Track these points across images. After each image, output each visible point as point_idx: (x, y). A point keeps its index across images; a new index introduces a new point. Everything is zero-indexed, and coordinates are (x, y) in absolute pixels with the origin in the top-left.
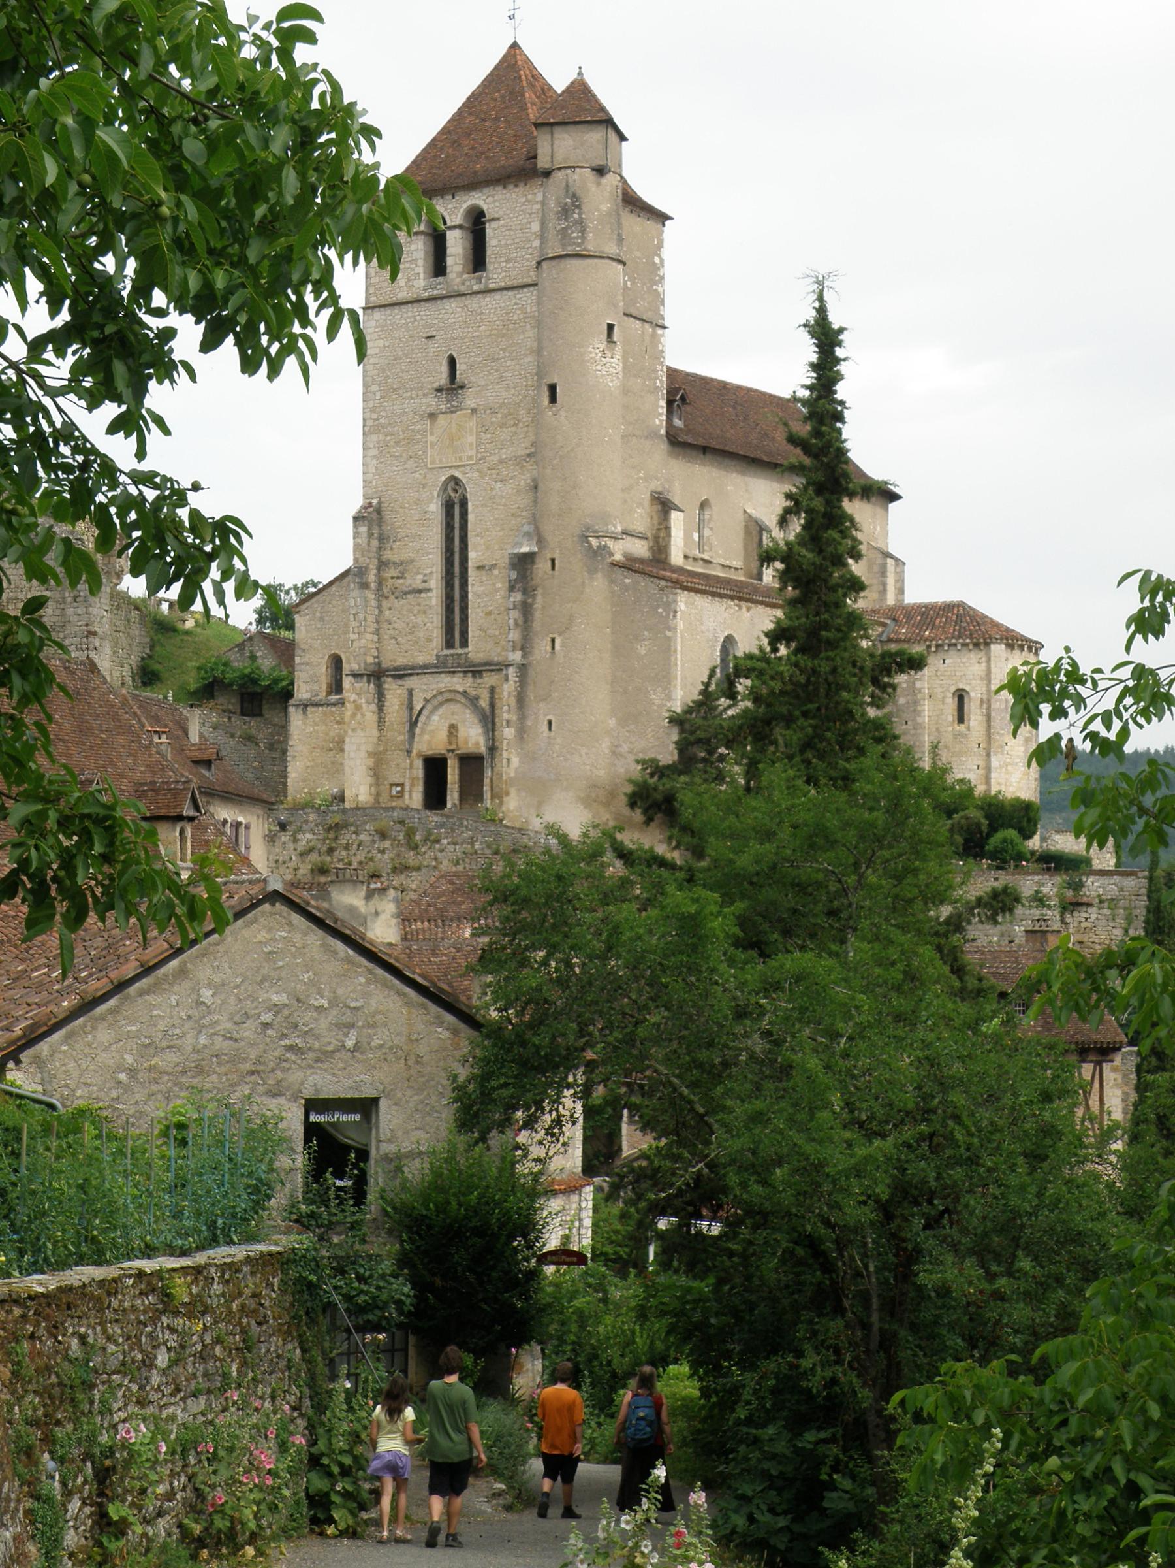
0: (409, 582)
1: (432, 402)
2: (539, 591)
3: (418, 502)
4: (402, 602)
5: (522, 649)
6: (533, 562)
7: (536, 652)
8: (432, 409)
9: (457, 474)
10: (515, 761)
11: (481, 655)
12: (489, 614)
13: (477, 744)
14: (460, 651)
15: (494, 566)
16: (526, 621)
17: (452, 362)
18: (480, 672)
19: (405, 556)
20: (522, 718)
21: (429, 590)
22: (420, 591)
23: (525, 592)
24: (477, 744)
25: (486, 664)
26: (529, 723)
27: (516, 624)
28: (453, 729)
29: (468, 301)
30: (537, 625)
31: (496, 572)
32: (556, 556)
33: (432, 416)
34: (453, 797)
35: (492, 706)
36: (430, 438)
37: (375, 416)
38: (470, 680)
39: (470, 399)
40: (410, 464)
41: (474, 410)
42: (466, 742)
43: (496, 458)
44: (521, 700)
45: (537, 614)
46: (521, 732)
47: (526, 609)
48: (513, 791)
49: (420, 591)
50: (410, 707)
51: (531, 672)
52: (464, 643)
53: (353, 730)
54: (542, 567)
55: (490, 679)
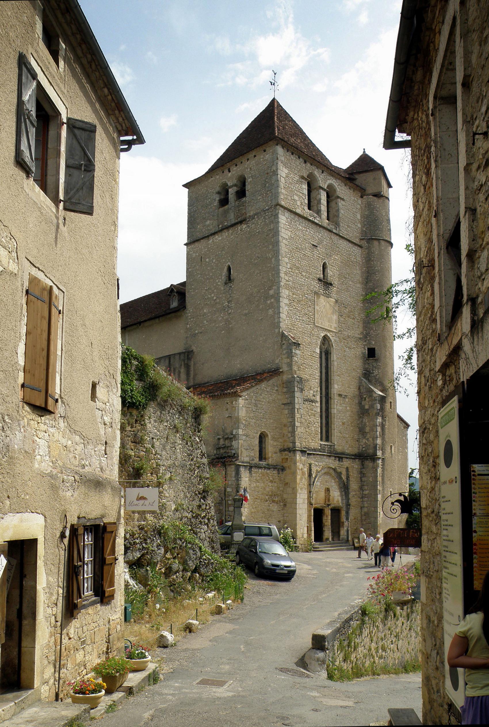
1: (316, 286)
2: (387, 419)
3: (310, 344)
5: (382, 450)
11: (340, 448)
12: (343, 424)
13: (338, 501)
16: (383, 435)
18: (342, 458)
23: (383, 417)
24: (338, 501)
28: (328, 490)
31: (347, 400)
34: (327, 533)
35: (348, 477)
38: (337, 462)
42: (333, 501)
45: (387, 430)
49: (312, 401)
50: (310, 475)
53: (301, 489)
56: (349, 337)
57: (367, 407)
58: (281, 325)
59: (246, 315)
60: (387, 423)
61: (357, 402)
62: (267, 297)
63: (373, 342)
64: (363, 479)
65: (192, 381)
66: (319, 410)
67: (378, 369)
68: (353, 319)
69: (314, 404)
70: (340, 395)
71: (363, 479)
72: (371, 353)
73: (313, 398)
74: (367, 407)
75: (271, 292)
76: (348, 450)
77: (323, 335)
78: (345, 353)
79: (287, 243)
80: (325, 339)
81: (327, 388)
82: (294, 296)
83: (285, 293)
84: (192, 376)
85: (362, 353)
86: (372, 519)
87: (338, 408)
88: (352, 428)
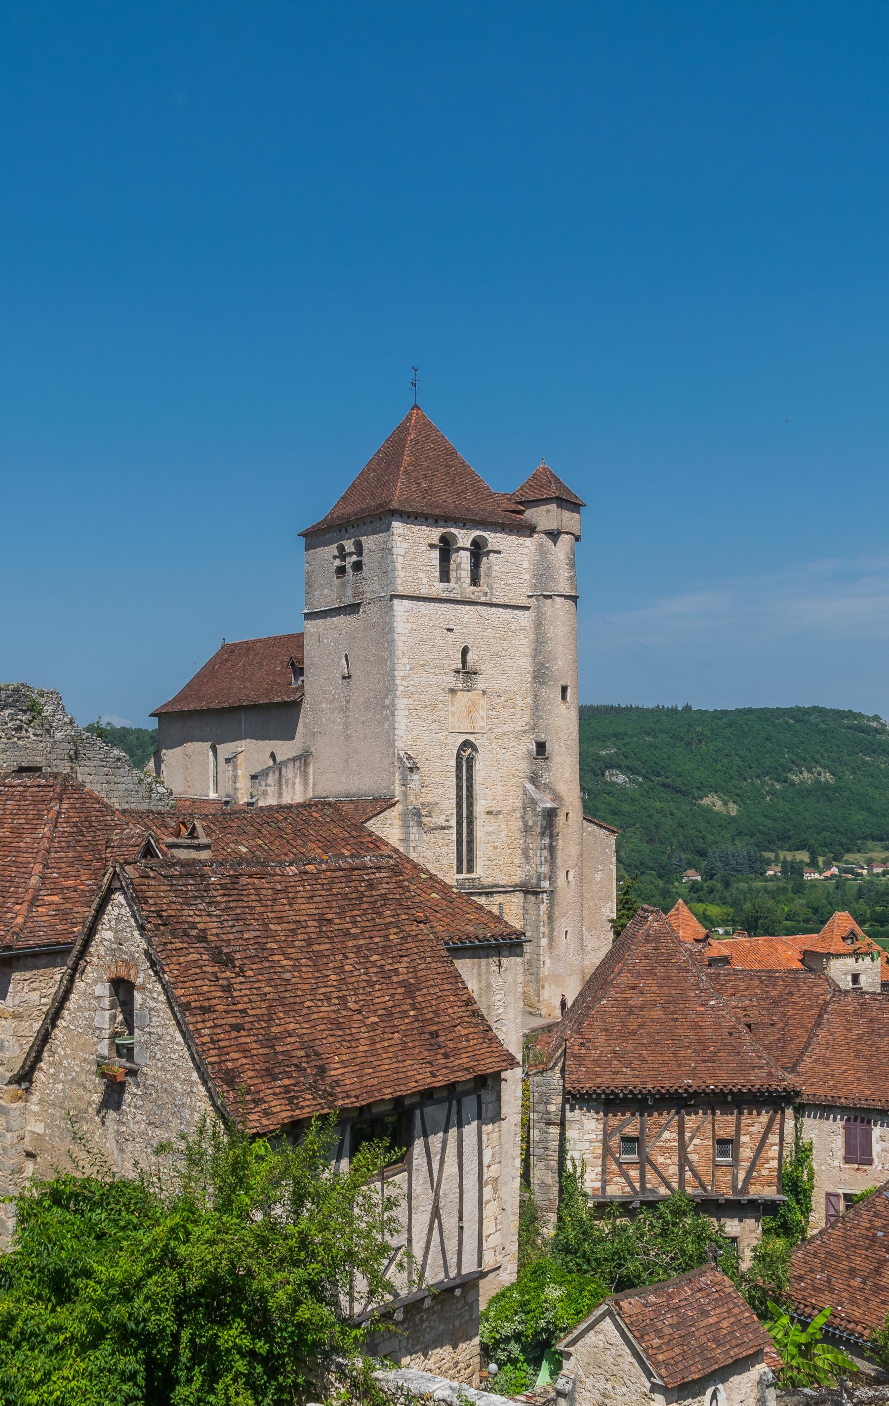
0: (435, 820)
1: (451, 680)
4: (430, 836)
5: (550, 879)
6: (556, 815)
7: (559, 881)
8: (452, 686)
9: (471, 738)
10: (548, 962)
12: (495, 848)
14: (469, 876)
15: (499, 812)
16: (551, 859)
17: (465, 651)
19: (430, 799)
20: (552, 930)
21: (451, 827)
22: (444, 828)
23: (551, 837)
25: (492, 887)
26: (555, 934)
27: (546, 860)
29: (478, 608)
30: (559, 861)
31: (501, 816)
32: (570, 812)
33: (453, 691)
36: (451, 708)
37: (405, 683)
39: (481, 683)
40: (434, 726)
41: (484, 692)
43: (500, 730)
44: (551, 918)
46: (551, 939)
47: (552, 849)
48: (546, 985)
49: (444, 828)
51: (557, 897)
52: (470, 870)
54: (560, 819)
55: (498, 899)
56: (504, 734)
57: (530, 823)
58: (397, 744)
59: (363, 723)
60: (560, 842)
61: (519, 816)
62: (384, 707)
63: (543, 736)
64: (526, 916)
65: (311, 790)
66: (454, 837)
67: (549, 771)
68: (514, 707)
69: (446, 831)
70: (489, 813)
71: (526, 916)
72: (541, 747)
73: (444, 824)
74: (530, 823)
75: (387, 702)
76: (502, 880)
77: (461, 741)
78: (499, 757)
79: (405, 639)
80: (467, 744)
81: (470, 805)
82: (417, 703)
83: (402, 703)
84: (311, 786)
85: (528, 751)
86: (535, 969)
87: (486, 828)
88: (509, 851)
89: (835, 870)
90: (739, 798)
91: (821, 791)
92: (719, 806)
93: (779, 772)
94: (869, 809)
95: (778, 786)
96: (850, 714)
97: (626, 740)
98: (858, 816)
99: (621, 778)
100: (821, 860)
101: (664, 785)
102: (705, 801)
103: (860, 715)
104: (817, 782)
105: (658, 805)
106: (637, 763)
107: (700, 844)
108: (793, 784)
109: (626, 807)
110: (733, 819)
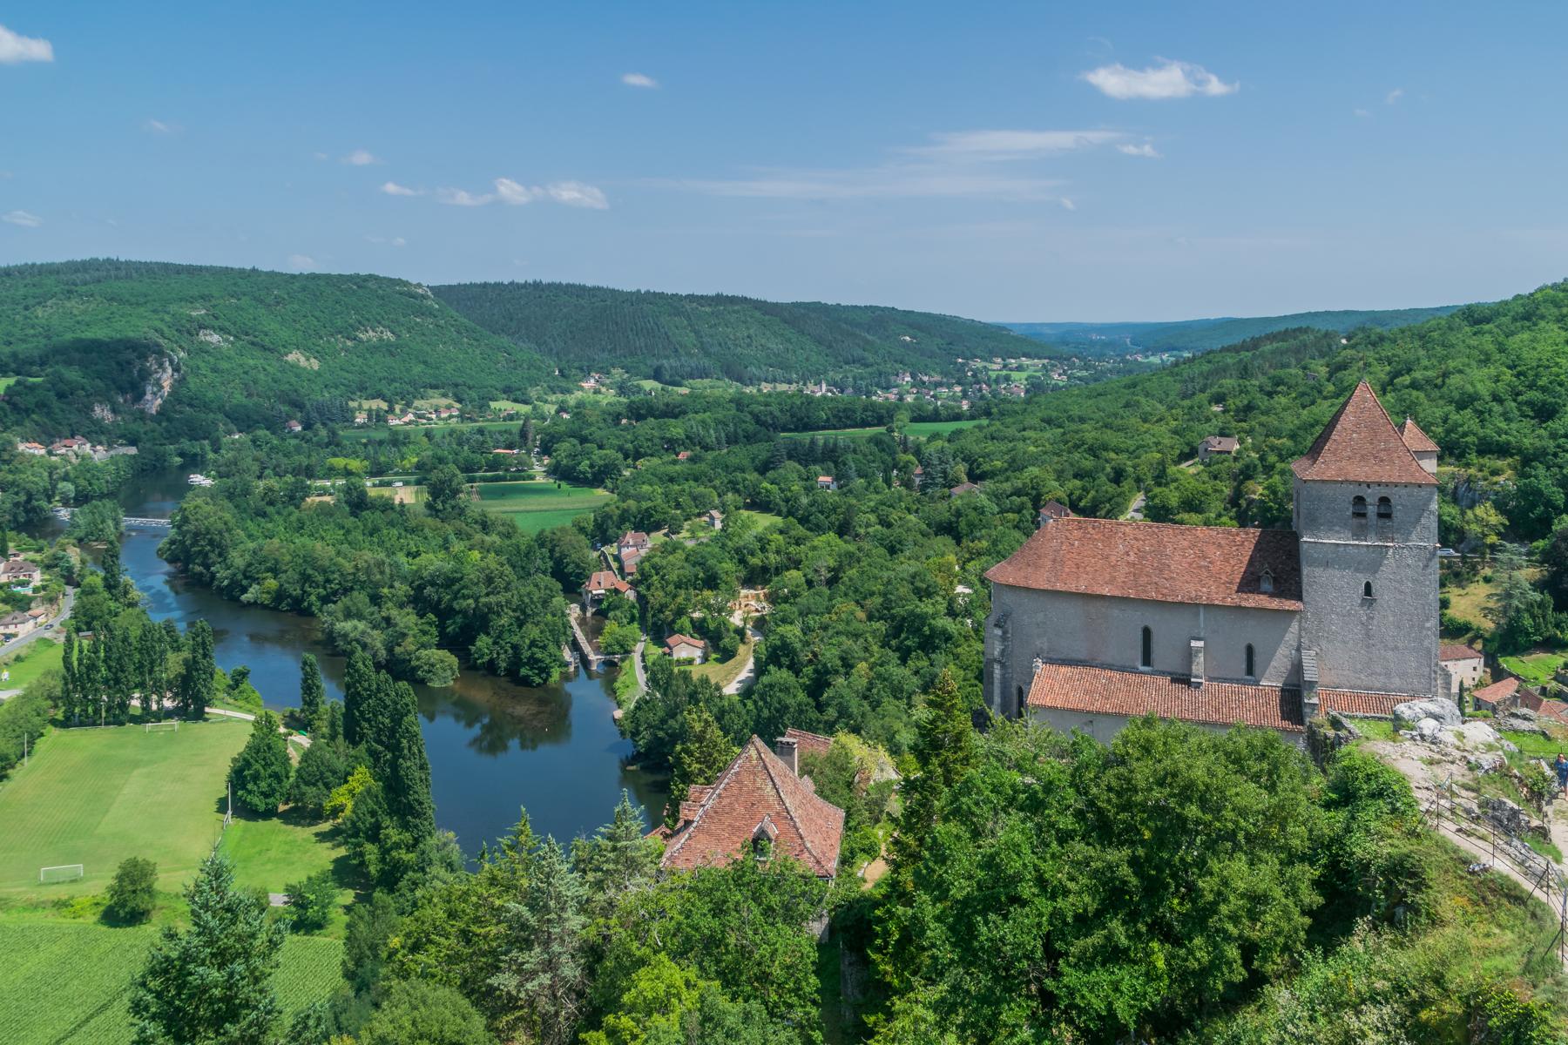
89: (410, 417)
90: (320, 355)
91: (390, 350)
92: (303, 362)
93: (348, 332)
94: (425, 363)
95: (349, 343)
96: (400, 282)
97: (214, 302)
98: (418, 369)
99: (215, 338)
100: (398, 408)
101: (253, 344)
102: (291, 358)
103: (406, 284)
104: (381, 339)
105: (251, 362)
106: (227, 324)
107: (294, 396)
108: (361, 341)
109: (224, 365)
110: (318, 374)
